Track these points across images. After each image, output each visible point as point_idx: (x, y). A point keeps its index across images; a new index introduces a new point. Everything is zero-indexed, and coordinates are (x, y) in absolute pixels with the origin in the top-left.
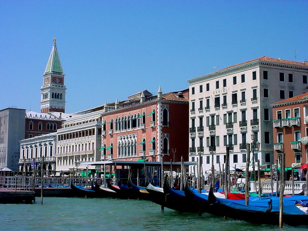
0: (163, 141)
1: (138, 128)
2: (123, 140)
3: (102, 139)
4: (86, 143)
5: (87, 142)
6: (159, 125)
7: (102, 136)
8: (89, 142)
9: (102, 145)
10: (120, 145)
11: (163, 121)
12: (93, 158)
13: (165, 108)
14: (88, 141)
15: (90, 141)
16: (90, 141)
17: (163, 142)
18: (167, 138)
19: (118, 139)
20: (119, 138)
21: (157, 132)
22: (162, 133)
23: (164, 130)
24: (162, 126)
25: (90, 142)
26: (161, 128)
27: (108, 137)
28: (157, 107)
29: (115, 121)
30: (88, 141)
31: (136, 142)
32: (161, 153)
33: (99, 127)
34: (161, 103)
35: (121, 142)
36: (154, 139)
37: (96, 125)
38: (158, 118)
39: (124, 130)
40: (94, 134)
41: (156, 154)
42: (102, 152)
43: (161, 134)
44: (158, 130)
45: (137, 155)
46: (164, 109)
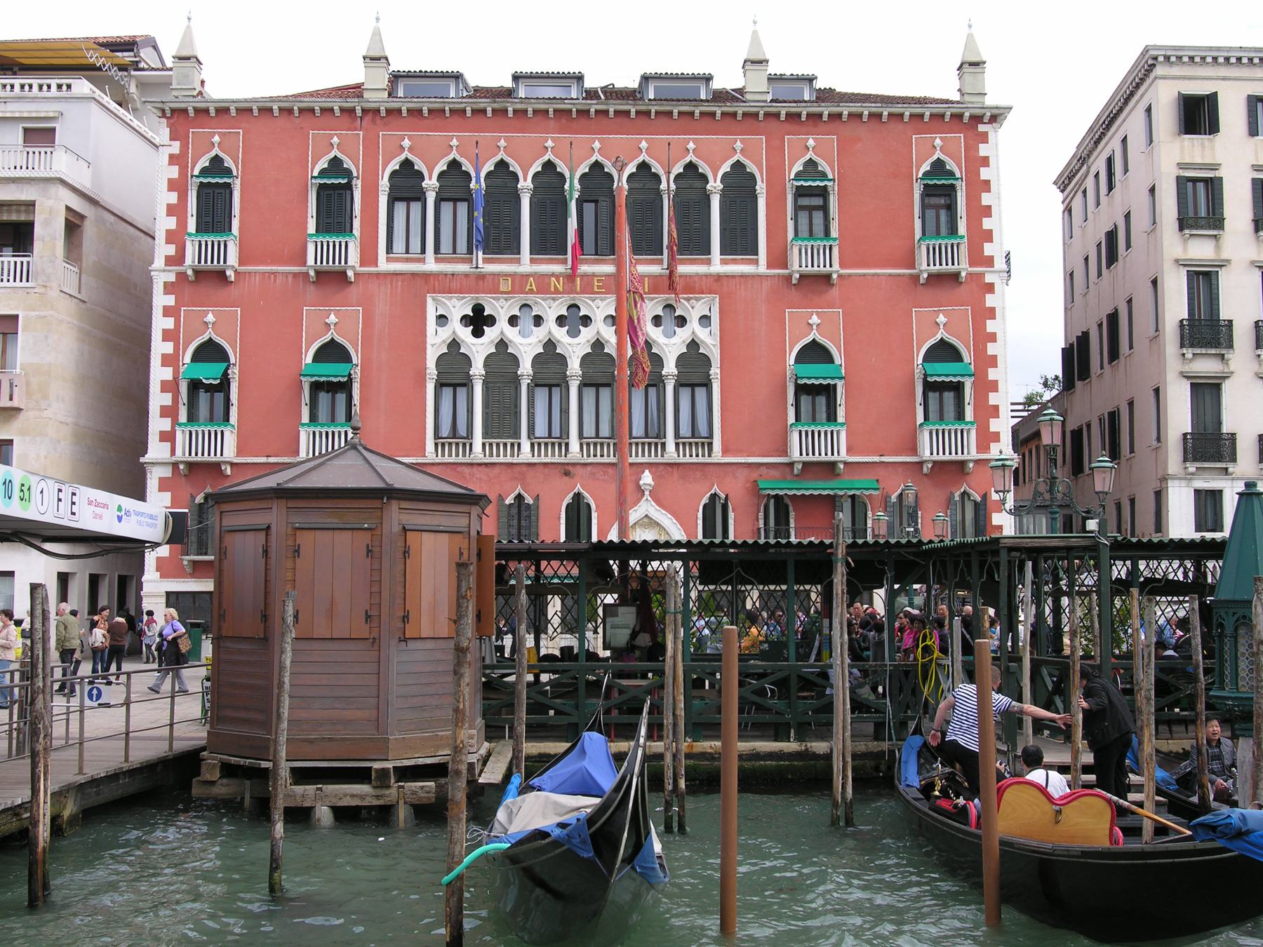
3: (161, 300)
7: (161, 276)
10: (454, 357)
28: (971, 149)
29: (384, 183)
31: (693, 358)
35: (479, 349)
45: (726, 451)
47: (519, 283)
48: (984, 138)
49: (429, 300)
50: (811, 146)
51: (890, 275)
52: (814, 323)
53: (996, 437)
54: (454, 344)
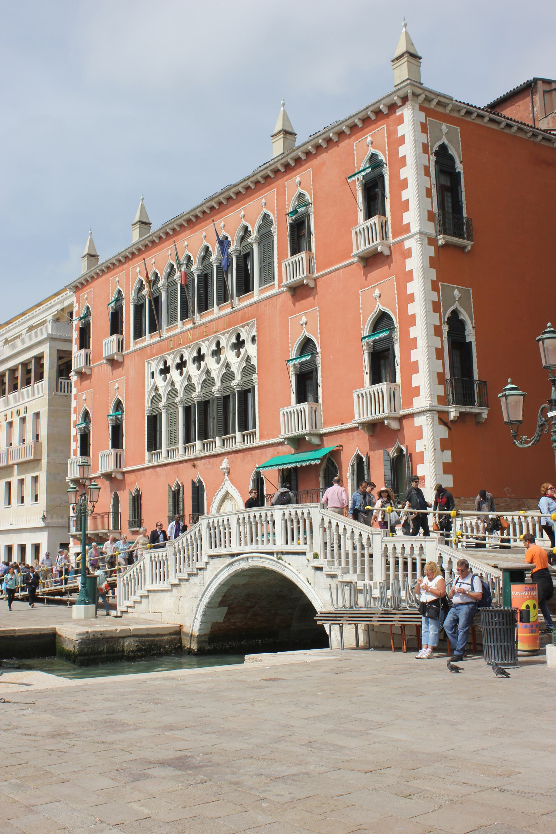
0: (445, 328)
1: (261, 292)
2: (174, 374)
4: (9, 420)
5: (15, 414)
6: (420, 233)
8: (22, 415)
9: (74, 417)
10: (156, 398)
11: (436, 210)
12: (36, 479)
13: (444, 140)
14: (18, 412)
15: (26, 408)
16: (26, 408)
17: (445, 335)
18: (464, 316)
19: (148, 375)
20: (155, 366)
21: (409, 276)
22: (441, 276)
23: (446, 263)
24: (432, 241)
25: (26, 412)
26: (431, 251)
27: (100, 368)
28: (391, 133)
30: (18, 412)
31: (248, 370)
32: (442, 400)
33: (63, 346)
34: (422, 108)
36: (382, 321)
37: (51, 338)
38: (410, 194)
39: (179, 322)
40: (40, 377)
41: (403, 412)
42: (75, 446)
43: (435, 287)
44: (416, 260)
45: (261, 437)
46: (436, 148)
47: (179, 341)
48: (400, 120)
49: (146, 364)
50: (298, 183)
51: (346, 266)
52: (305, 322)
53: (416, 392)
54: (156, 389)
